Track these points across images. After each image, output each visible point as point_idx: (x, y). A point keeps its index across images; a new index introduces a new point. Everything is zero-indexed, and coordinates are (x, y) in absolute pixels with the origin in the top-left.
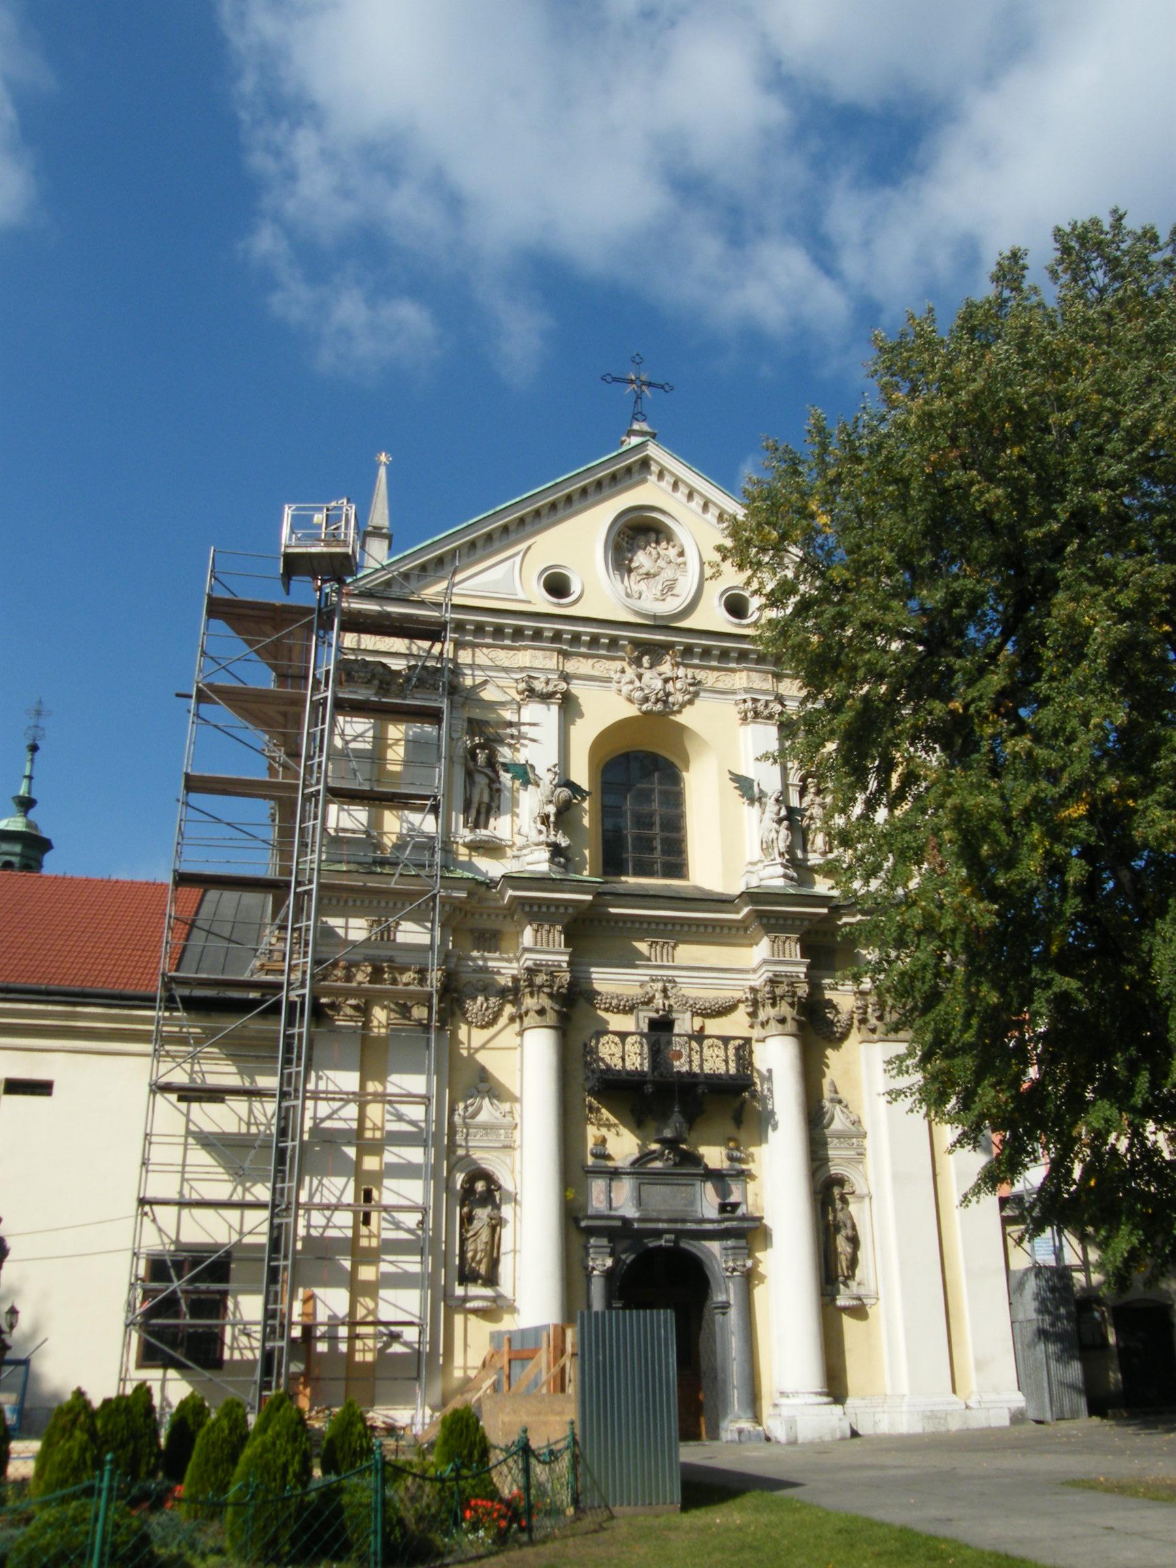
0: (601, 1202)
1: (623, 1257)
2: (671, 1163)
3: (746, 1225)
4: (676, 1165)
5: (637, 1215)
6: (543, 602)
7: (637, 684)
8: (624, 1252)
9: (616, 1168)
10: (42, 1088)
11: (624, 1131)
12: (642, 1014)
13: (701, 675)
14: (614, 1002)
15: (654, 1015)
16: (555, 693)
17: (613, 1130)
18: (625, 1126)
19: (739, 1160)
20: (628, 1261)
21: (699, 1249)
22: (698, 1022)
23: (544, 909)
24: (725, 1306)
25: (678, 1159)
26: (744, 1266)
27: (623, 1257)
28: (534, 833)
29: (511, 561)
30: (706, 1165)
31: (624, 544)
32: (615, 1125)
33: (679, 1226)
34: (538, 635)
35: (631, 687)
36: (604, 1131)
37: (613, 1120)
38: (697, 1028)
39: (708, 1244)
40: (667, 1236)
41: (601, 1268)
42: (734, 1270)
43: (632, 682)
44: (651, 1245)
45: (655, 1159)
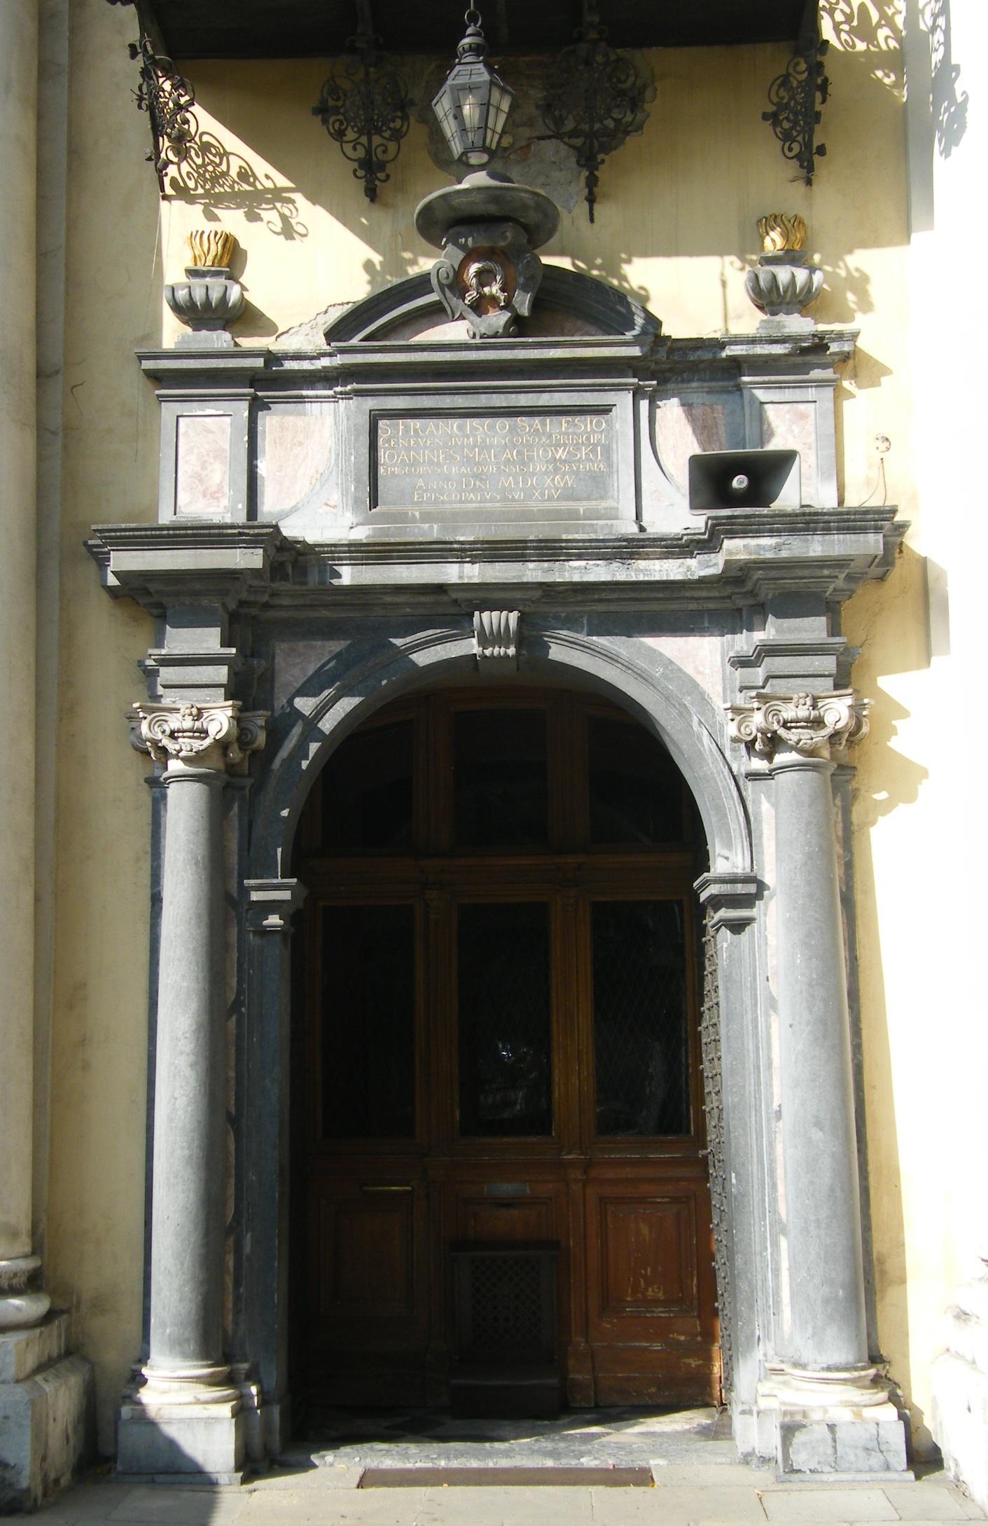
0: (214, 496)
1: (305, 705)
2: (497, 319)
3: (816, 547)
4: (519, 326)
5: (361, 534)
8: (306, 690)
9: (272, 358)
11: (307, 212)
17: (270, 215)
18: (313, 198)
19: (803, 301)
20: (328, 724)
21: (628, 667)
25: (523, 303)
26: (818, 723)
27: (305, 705)
30: (653, 322)
32: (277, 195)
33: (533, 572)
36: (232, 221)
37: (266, 173)
39: (668, 646)
40: (489, 619)
41: (188, 745)
42: (773, 743)
44: (423, 658)
45: (436, 313)
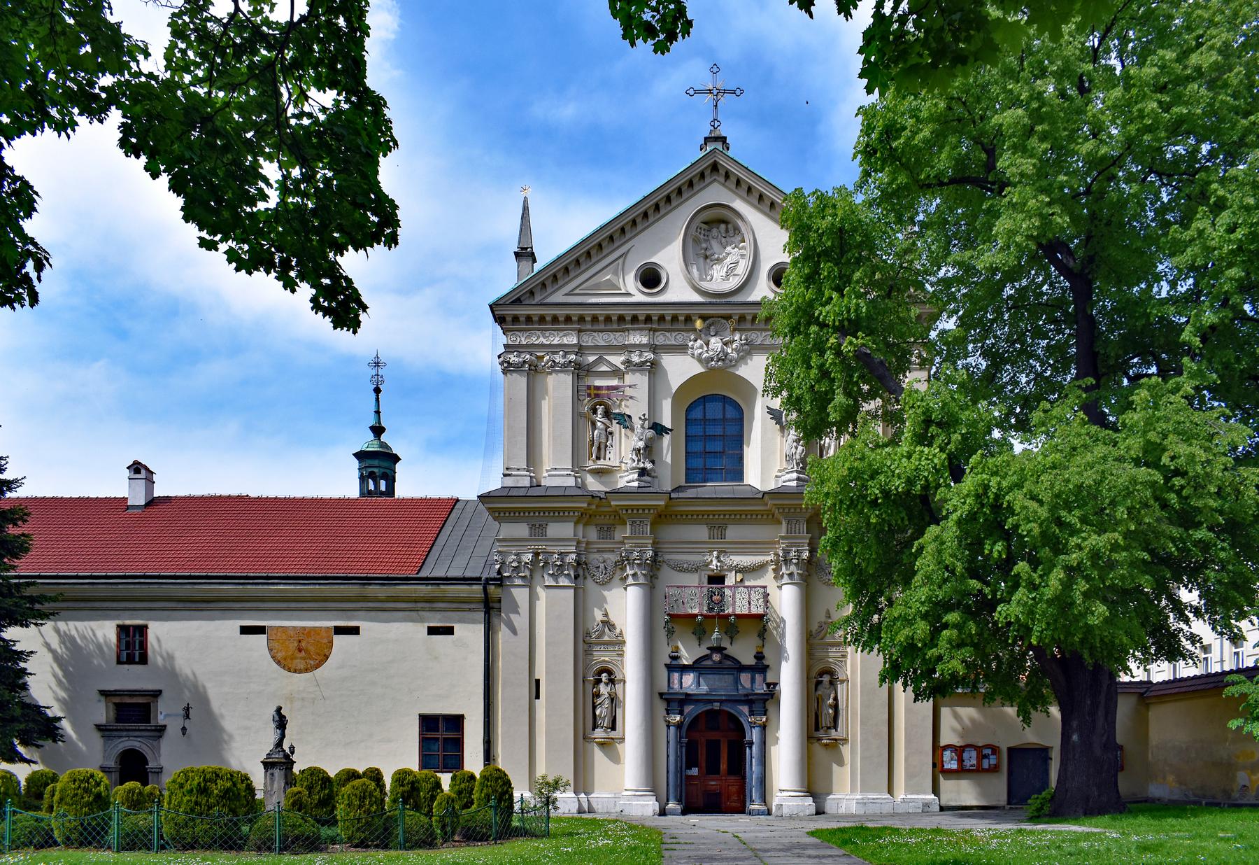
6: (637, 294)
7: (705, 348)
10: (355, 631)
12: (703, 573)
14: (685, 566)
15: (711, 573)
16: (646, 361)
22: (739, 576)
23: (635, 512)
24: (751, 743)
28: (629, 462)
34: (635, 319)
35: (700, 351)
38: (738, 580)
39: (741, 707)
43: (701, 347)
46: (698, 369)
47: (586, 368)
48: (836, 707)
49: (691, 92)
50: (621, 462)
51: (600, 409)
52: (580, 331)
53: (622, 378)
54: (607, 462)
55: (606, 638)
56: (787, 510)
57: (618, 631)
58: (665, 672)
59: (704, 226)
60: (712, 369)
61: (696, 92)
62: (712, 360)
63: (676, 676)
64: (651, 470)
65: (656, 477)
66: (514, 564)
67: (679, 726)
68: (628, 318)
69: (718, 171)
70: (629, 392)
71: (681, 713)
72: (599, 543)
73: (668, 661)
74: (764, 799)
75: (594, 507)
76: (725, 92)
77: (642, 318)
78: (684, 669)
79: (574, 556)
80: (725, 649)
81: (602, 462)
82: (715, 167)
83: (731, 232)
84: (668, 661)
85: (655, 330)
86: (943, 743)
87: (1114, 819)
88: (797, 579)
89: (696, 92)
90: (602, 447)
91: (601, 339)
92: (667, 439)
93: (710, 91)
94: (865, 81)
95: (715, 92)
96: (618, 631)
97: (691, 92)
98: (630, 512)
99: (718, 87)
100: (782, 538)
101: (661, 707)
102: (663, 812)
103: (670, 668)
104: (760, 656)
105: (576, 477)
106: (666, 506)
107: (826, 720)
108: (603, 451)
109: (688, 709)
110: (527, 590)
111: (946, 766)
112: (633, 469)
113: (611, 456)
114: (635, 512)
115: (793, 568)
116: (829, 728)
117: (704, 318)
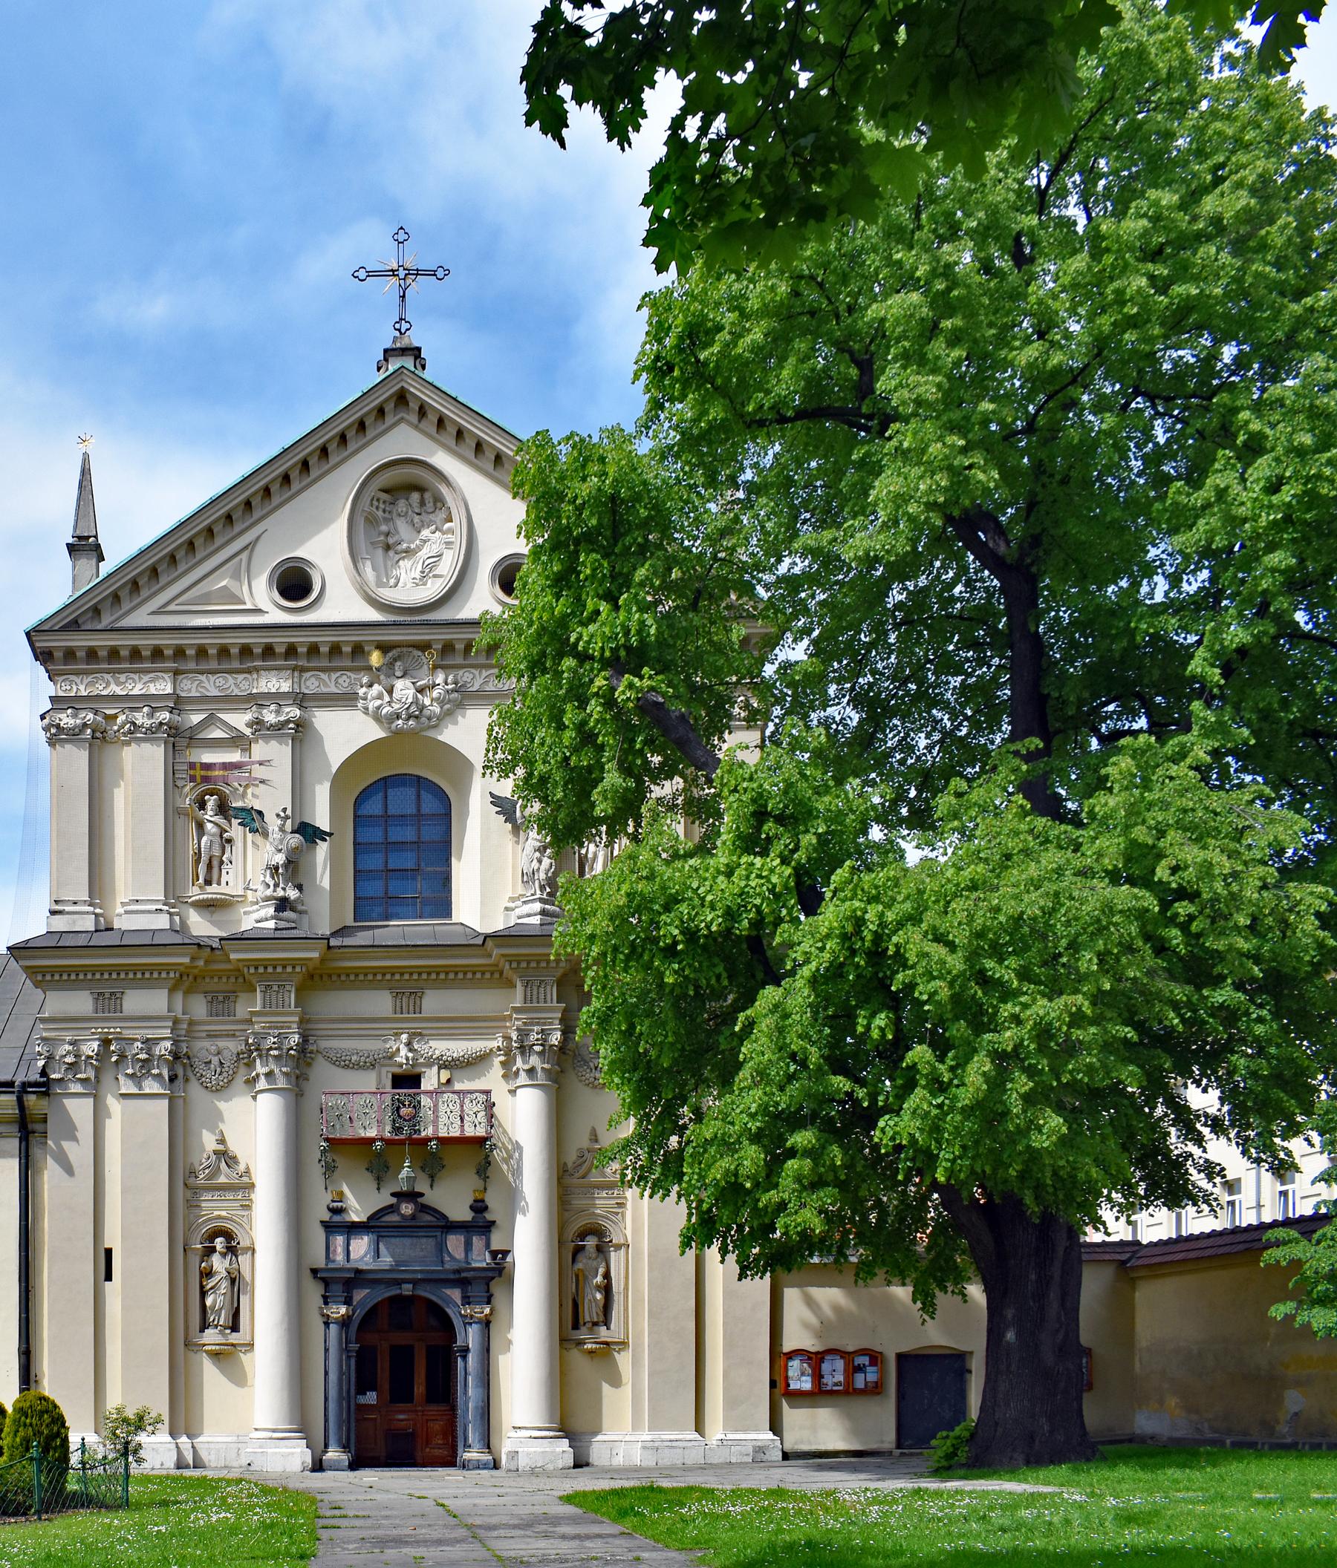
6: (273, 610)
7: (387, 698)
12: (384, 1070)
13: (465, 676)
14: (354, 1058)
15: (397, 1070)
16: (288, 721)
22: (445, 1075)
23: (270, 970)
24: (465, 1350)
28: (261, 888)
29: (237, 559)
31: (380, 513)
34: (268, 651)
35: (378, 702)
38: (443, 1080)
39: (448, 1292)
43: (380, 697)
46: (375, 732)
47: (187, 734)
48: (607, 1289)
49: (362, 274)
50: (247, 888)
51: (211, 802)
52: (176, 673)
53: (247, 750)
54: (223, 889)
55: (222, 1179)
56: (524, 965)
57: (242, 1168)
58: (320, 1234)
59: (384, 496)
60: (398, 733)
61: (370, 274)
62: (398, 717)
63: (339, 1240)
64: (296, 900)
65: (304, 912)
66: (69, 1059)
67: (345, 1323)
68: (258, 650)
69: (407, 404)
70: (259, 772)
71: (348, 1302)
72: (210, 1023)
73: (326, 1216)
74: (487, 1445)
75: (201, 963)
76: (418, 273)
77: (280, 650)
78: (352, 1229)
79: (168, 1044)
80: (422, 1195)
81: (214, 888)
82: (402, 398)
83: (430, 506)
84: (326, 1216)
85: (303, 670)
86: (788, 1346)
87: (1076, 1471)
88: (541, 1078)
89: (370, 274)
90: (215, 863)
91: (212, 685)
92: (322, 849)
93: (393, 273)
94: (653, 251)
95: (402, 273)
96: (242, 1168)
97: (362, 274)
98: (261, 970)
99: (408, 265)
100: (516, 1010)
101: (314, 1292)
102: (318, 1466)
103: (330, 1228)
104: (479, 1207)
105: (171, 914)
106: (323, 960)
107: (590, 1311)
108: (215, 871)
109: (359, 1295)
110: (89, 1102)
111: (794, 1385)
112: (267, 899)
113: (230, 878)
114: (270, 970)
115: (534, 1060)
116: (595, 1324)
117: (384, 648)
